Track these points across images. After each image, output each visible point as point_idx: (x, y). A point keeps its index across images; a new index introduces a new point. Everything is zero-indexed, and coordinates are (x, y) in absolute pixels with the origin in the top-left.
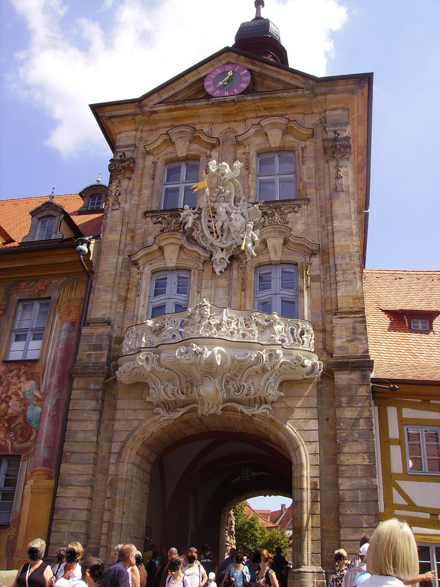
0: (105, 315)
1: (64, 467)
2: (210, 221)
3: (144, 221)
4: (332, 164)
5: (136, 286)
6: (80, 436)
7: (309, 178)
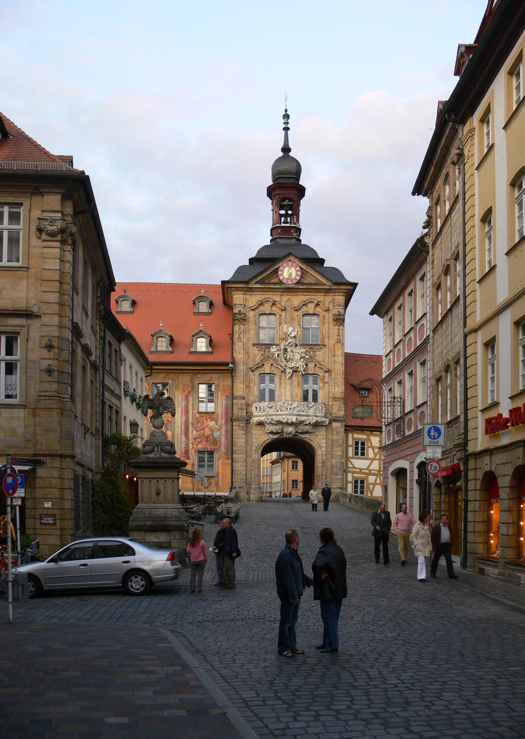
2: (284, 354)
3: (253, 348)
4: (337, 327)
6: (239, 444)
7: (326, 333)
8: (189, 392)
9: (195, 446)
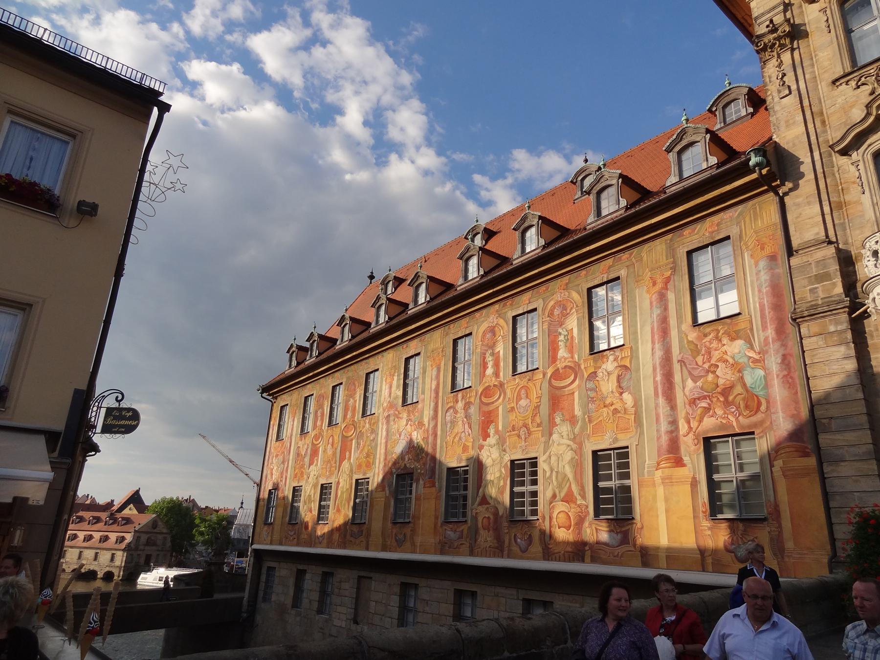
0: (818, 234)
1: (823, 439)
5: (854, 183)
8: (667, 281)
9: (694, 424)
